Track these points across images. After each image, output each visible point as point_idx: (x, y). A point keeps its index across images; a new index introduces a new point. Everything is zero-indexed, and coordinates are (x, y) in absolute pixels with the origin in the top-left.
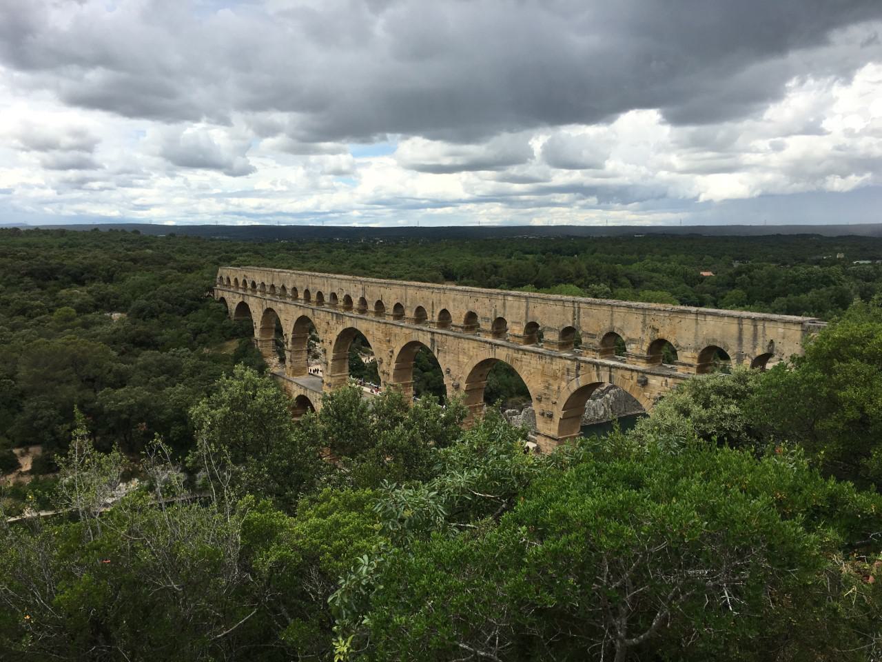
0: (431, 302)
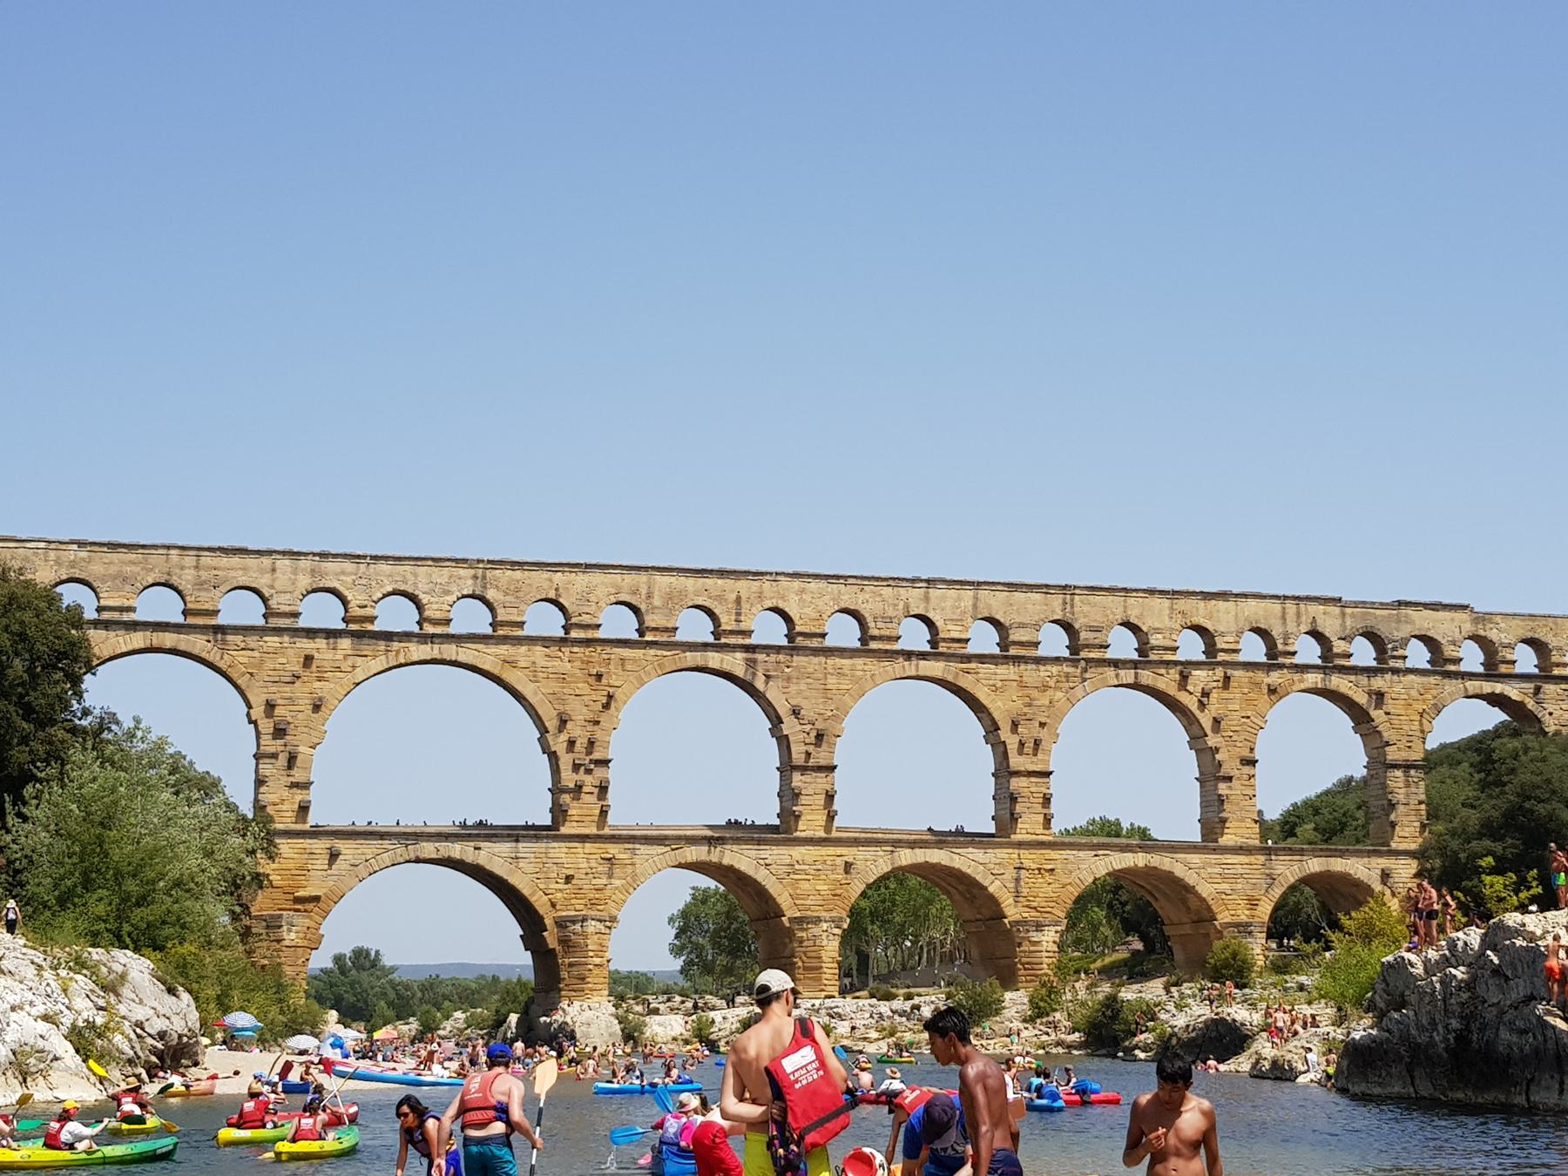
0: (734, 596)
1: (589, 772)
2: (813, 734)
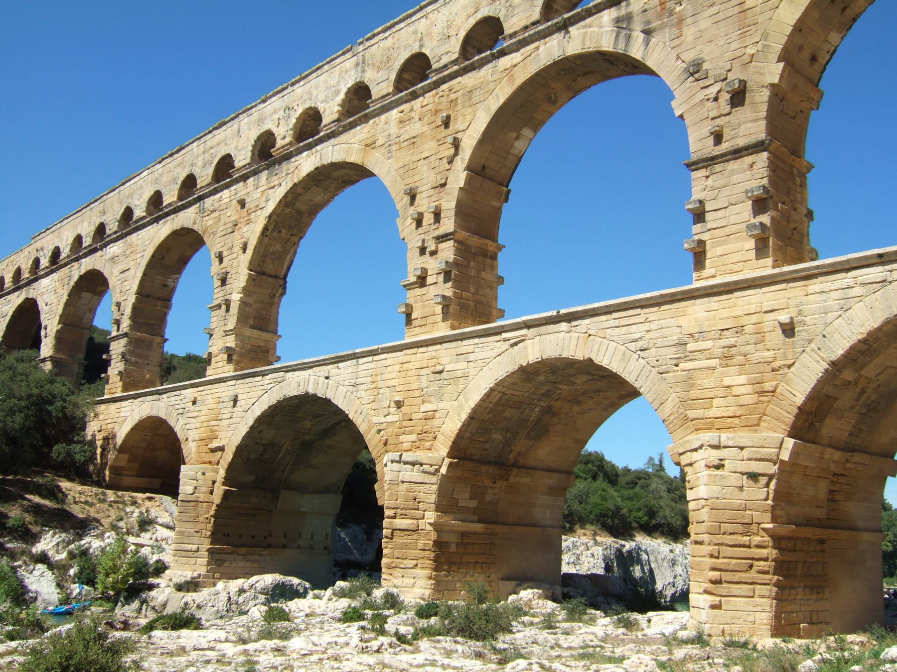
1: (433, 253)
2: (725, 97)
